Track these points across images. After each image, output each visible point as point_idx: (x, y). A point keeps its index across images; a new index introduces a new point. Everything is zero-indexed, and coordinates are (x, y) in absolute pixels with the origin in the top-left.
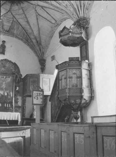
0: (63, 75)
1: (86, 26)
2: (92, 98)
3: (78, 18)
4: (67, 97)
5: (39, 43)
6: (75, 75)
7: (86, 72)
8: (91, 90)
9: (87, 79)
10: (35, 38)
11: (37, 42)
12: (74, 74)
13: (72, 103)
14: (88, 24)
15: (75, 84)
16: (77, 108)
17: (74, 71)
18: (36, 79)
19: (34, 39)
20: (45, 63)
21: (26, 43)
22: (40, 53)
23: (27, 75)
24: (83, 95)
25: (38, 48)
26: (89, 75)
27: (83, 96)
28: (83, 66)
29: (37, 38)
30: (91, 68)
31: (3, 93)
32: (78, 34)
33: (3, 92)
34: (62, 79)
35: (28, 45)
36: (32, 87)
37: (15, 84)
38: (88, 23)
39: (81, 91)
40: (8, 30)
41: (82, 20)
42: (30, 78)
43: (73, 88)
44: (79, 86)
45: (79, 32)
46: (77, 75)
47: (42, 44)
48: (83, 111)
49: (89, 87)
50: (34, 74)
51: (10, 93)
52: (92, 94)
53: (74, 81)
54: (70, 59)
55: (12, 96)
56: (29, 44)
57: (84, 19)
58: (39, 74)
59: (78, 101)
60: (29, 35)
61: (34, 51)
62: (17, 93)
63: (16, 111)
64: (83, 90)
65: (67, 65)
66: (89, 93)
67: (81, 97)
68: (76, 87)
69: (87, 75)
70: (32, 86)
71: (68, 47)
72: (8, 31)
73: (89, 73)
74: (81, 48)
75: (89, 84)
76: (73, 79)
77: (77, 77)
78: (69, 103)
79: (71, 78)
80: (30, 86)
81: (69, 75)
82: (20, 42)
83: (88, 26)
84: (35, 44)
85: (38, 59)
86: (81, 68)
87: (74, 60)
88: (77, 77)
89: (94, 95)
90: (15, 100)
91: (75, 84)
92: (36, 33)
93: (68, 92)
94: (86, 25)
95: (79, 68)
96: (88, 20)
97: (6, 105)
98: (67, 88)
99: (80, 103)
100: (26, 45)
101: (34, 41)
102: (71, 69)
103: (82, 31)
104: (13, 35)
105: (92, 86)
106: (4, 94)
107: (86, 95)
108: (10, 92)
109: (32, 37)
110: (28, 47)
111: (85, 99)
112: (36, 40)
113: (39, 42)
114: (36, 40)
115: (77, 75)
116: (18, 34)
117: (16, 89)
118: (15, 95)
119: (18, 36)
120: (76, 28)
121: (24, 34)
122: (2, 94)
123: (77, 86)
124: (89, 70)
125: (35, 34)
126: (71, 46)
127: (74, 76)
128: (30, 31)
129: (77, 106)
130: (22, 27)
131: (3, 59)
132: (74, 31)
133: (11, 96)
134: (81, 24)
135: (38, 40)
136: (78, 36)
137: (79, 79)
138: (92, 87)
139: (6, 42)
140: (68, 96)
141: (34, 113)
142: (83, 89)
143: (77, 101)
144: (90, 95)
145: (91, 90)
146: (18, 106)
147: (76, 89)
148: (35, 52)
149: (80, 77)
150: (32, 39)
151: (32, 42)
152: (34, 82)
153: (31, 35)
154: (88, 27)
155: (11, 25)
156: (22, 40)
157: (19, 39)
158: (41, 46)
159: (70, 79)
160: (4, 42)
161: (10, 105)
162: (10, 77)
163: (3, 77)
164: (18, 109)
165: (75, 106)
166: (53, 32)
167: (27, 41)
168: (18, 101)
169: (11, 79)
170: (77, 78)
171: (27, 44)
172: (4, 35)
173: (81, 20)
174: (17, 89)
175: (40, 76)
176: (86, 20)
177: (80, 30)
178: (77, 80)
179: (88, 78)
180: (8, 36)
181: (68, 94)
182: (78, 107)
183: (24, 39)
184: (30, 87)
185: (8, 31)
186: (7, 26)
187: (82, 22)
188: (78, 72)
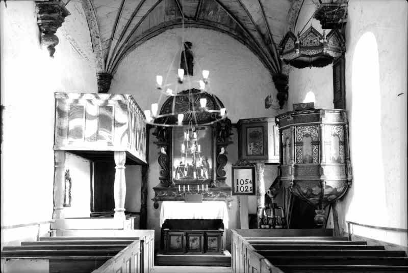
0: (288, 138)
1: (340, 21)
2: (347, 184)
3: (319, 4)
4: (293, 183)
5: (268, 41)
6: (309, 139)
7: (336, 131)
8: (346, 166)
9: (338, 143)
10: (258, 29)
11: (263, 36)
12: (307, 135)
13: (305, 194)
14: (345, 14)
15: (308, 158)
16: (317, 202)
17: (307, 130)
18: (260, 130)
19: (255, 31)
20: (288, 83)
21: (241, 39)
22: (273, 61)
23: (240, 120)
24: (321, 179)
25: (266, 50)
26: (343, 134)
27: (323, 181)
28: (323, 119)
29: (261, 26)
30: (347, 120)
31: (193, 163)
32: (315, 48)
33: (192, 161)
34: (286, 145)
35: (245, 43)
36: (252, 147)
37: (217, 142)
38: (345, 12)
39: (319, 170)
40: (194, 15)
41: (328, 10)
42: (247, 128)
43: (303, 166)
44: (315, 161)
45: (317, 44)
46: (312, 139)
47: (275, 40)
48: (338, 207)
49: (342, 161)
50: (254, 119)
51: (207, 162)
52: (347, 175)
53: (307, 150)
54: (296, 108)
55: (211, 167)
56: (248, 42)
57: (333, 8)
58: (264, 118)
59: (316, 190)
60: (242, 22)
61: (260, 57)
62: (221, 161)
63: (221, 199)
64: (322, 170)
65: (292, 118)
66: (340, 173)
67: (320, 184)
68: (310, 163)
69: (338, 136)
70: (252, 144)
71: (309, 68)
72: (194, 19)
73: (341, 130)
74: (334, 68)
75: (342, 154)
76: (304, 147)
77: (314, 143)
78: (299, 194)
79: (301, 144)
80: (249, 147)
81: (296, 139)
82: (226, 37)
83: (345, 21)
84: (260, 41)
85: (272, 75)
86: (320, 124)
87: (305, 110)
88: (314, 143)
89: (352, 178)
90: (217, 176)
91: (308, 158)
92: (257, 17)
93: (293, 172)
94: (339, 20)
95: (317, 125)
96: (345, 6)
97: (201, 187)
98: (291, 166)
99: (322, 193)
100: (241, 43)
101: (256, 34)
102: (299, 126)
103: (326, 41)
104: (208, 25)
105: (349, 159)
106: (195, 165)
107: (331, 177)
108: (206, 160)
109: (250, 27)
110: (245, 47)
111: (329, 187)
112: (259, 31)
113: (267, 37)
114: (259, 31)
115: (312, 139)
116: (219, 21)
117: (218, 151)
118: (218, 165)
119: (218, 26)
120: (312, 34)
121: (231, 21)
122: (191, 164)
123: (312, 161)
124: (344, 125)
125: (255, 19)
126: (314, 66)
127: (307, 141)
128: (241, 14)
129: (317, 198)
130: (224, 7)
131: (188, 90)
132: (307, 41)
133: (208, 166)
134: (326, 18)
135: (264, 31)
136: (314, 52)
137: (315, 147)
138: (348, 161)
139: (193, 44)
140: (294, 181)
141: (260, 201)
142: (323, 167)
143: (314, 189)
144: (344, 176)
145: (346, 166)
146: (224, 186)
147: (311, 166)
148: (262, 59)
149: (318, 143)
150: (249, 31)
151: (252, 36)
152: (255, 136)
153: (246, 22)
154: (345, 23)
155: (199, 4)
156: (229, 33)
157: (223, 31)
158: (273, 45)
159: (299, 146)
160: (188, 44)
161: (207, 186)
162: (203, 128)
163: (191, 130)
164: (225, 194)
165: (312, 199)
166: (296, 11)
167: (241, 33)
168: (226, 178)
169: (207, 132)
170: (312, 145)
171: (241, 41)
172: (187, 27)
173: (324, 9)
174: (220, 151)
175: (266, 122)
176: (340, 7)
177: (320, 39)
178: (313, 149)
179: (340, 142)
180: (197, 27)
181: (293, 177)
182: (320, 201)
183: (233, 32)
184: (247, 146)
185: (194, 19)
186: (190, 7)
187: (329, 14)
188: (314, 133)
